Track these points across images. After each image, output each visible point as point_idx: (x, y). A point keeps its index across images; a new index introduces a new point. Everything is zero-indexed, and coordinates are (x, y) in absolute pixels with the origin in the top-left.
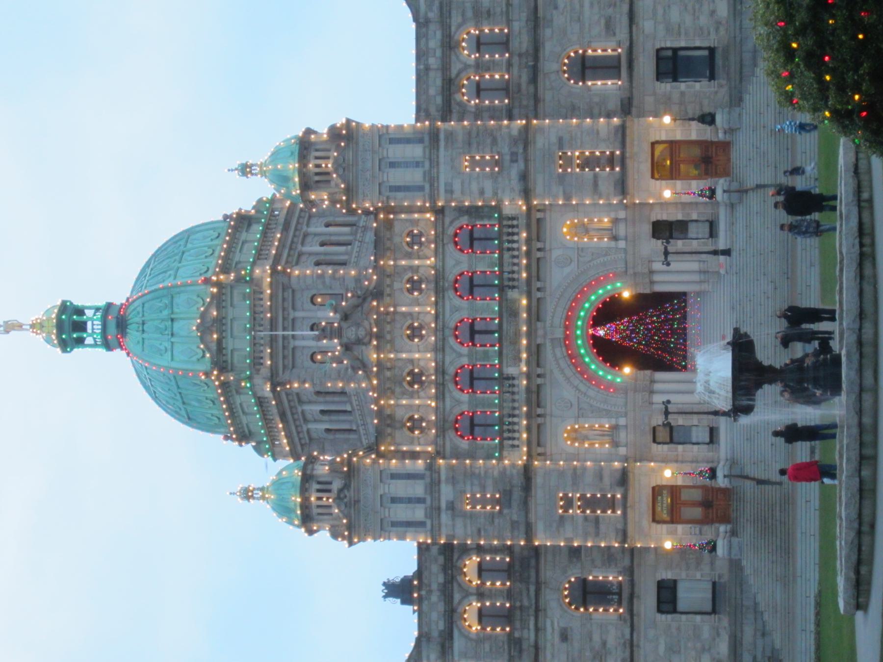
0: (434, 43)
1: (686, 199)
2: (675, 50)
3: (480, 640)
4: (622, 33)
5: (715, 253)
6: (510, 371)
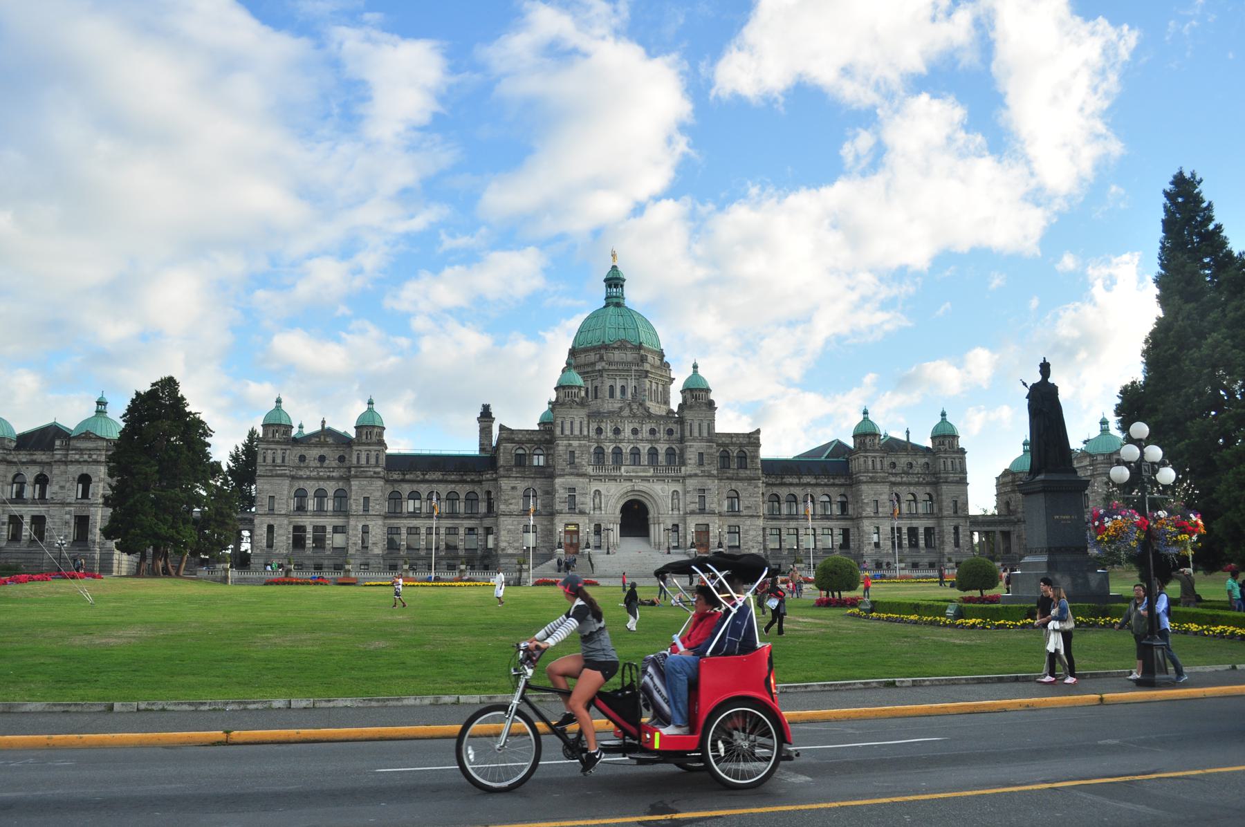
1: (689, 538)
4: (745, 513)
6: (623, 468)
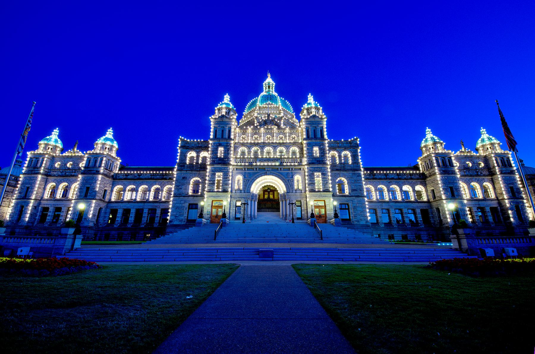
0: (345, 145)
2: (348, 209)
3: (185, 157)
5: (293, 219)
